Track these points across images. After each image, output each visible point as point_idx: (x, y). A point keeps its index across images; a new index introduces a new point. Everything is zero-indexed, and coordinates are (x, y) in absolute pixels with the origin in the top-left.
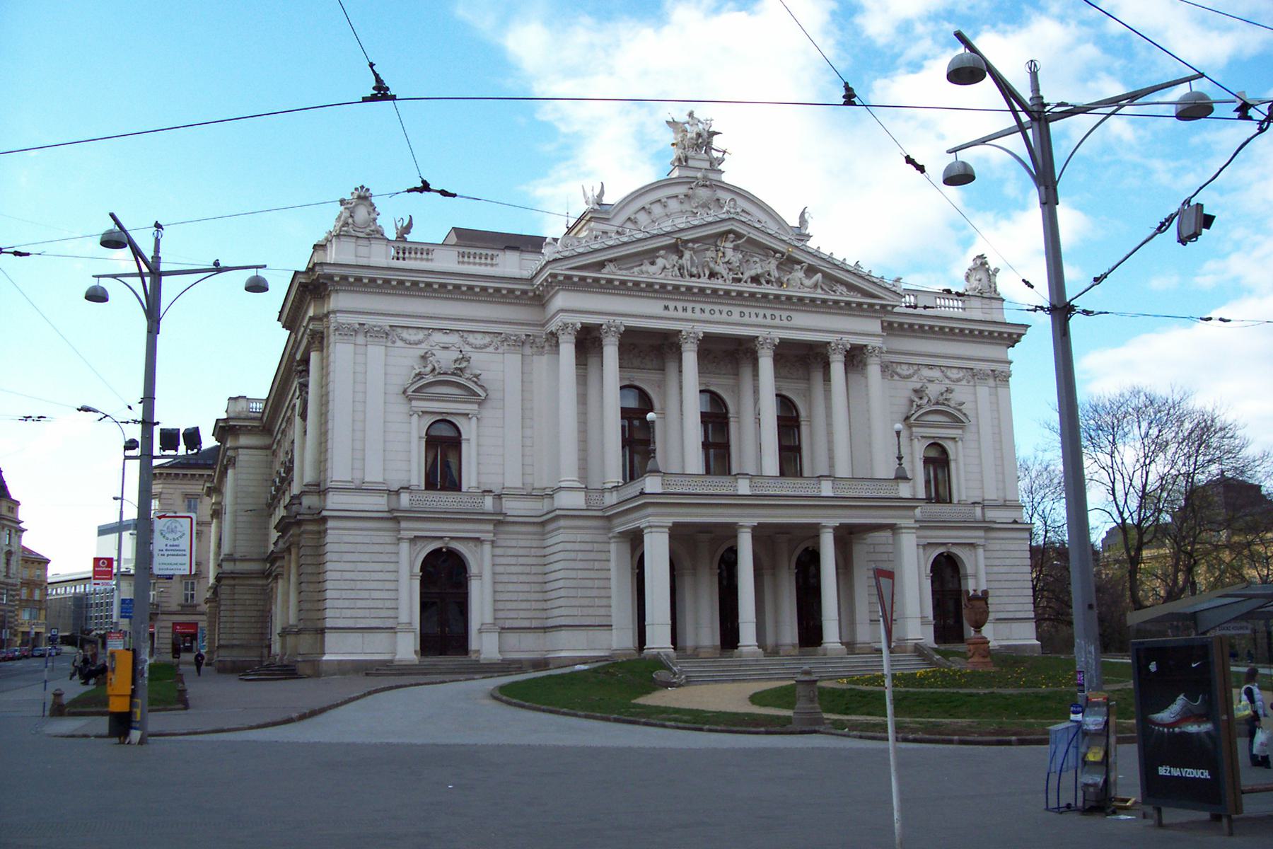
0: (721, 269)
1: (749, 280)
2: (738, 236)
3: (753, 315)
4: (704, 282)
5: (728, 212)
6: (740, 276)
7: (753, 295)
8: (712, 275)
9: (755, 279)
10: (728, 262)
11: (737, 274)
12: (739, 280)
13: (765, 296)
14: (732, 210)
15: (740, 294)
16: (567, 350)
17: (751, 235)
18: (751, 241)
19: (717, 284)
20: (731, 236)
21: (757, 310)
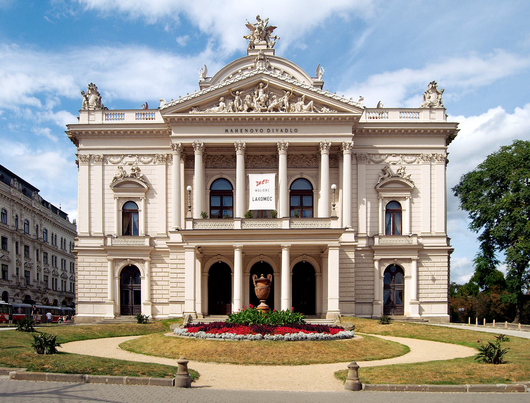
0: (255, 105)
1: (272, 110)
2: (265, 84)
3: (275, 131)
4: (244, 113)
5: (259, 70)
6: (266, 108)
7: (272, 119)
8: (250, 109)
9: (275, 109)
10: (259, 101)
11: (264, 107)
12: (266, 110)
13: (280, 119)
14: (261, 69)
15: (265, 119)
16: (176, 158)
17: (270, 82)
18: (271, 86)
19: (253, 114)
20: (261, 84)
21: (277, 128)
